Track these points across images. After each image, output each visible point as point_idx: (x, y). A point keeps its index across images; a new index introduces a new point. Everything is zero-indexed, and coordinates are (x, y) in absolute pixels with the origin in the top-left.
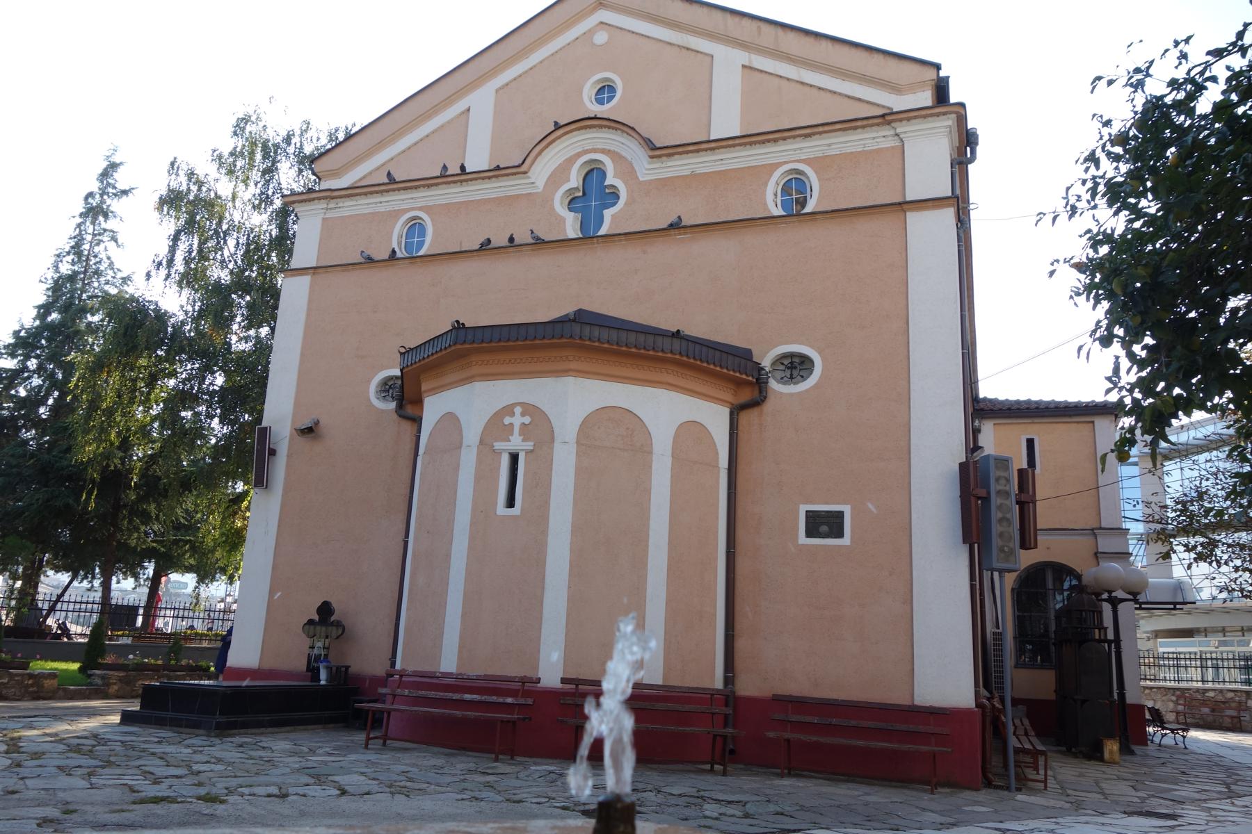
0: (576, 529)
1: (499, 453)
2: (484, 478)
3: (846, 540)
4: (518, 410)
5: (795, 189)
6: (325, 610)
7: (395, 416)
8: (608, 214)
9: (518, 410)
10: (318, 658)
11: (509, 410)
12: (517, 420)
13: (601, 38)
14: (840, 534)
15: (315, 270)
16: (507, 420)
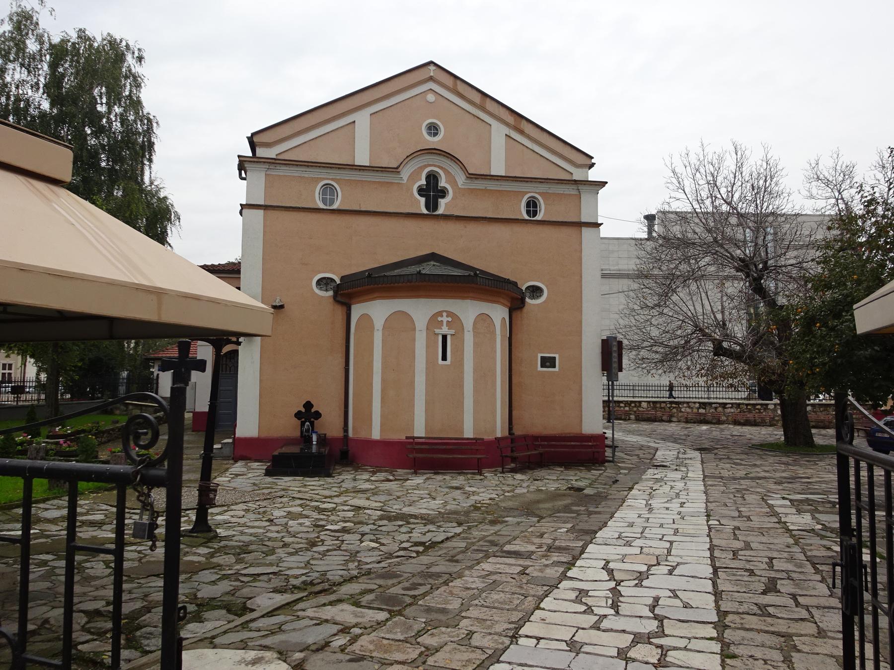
0: (475, 370)
1: (438, 334)
2: (430, 346)
3: (557, 369)
4: (445, 314)
5: (532, 206)
6: (308, 405)
7: (332, 300)
8: (442, 202)
9: (445, 314)
10: (307, 431)
11: (440, 314)
12: (445, 319)
13: (431, 97)
14: (554, 367)
15: (265, 207)
16: (440, 319)
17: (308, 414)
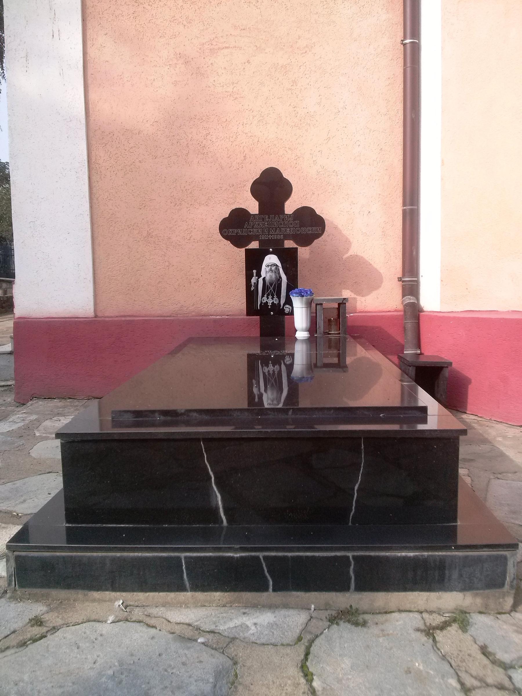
10: (273, 288)
17: (273, 225)
